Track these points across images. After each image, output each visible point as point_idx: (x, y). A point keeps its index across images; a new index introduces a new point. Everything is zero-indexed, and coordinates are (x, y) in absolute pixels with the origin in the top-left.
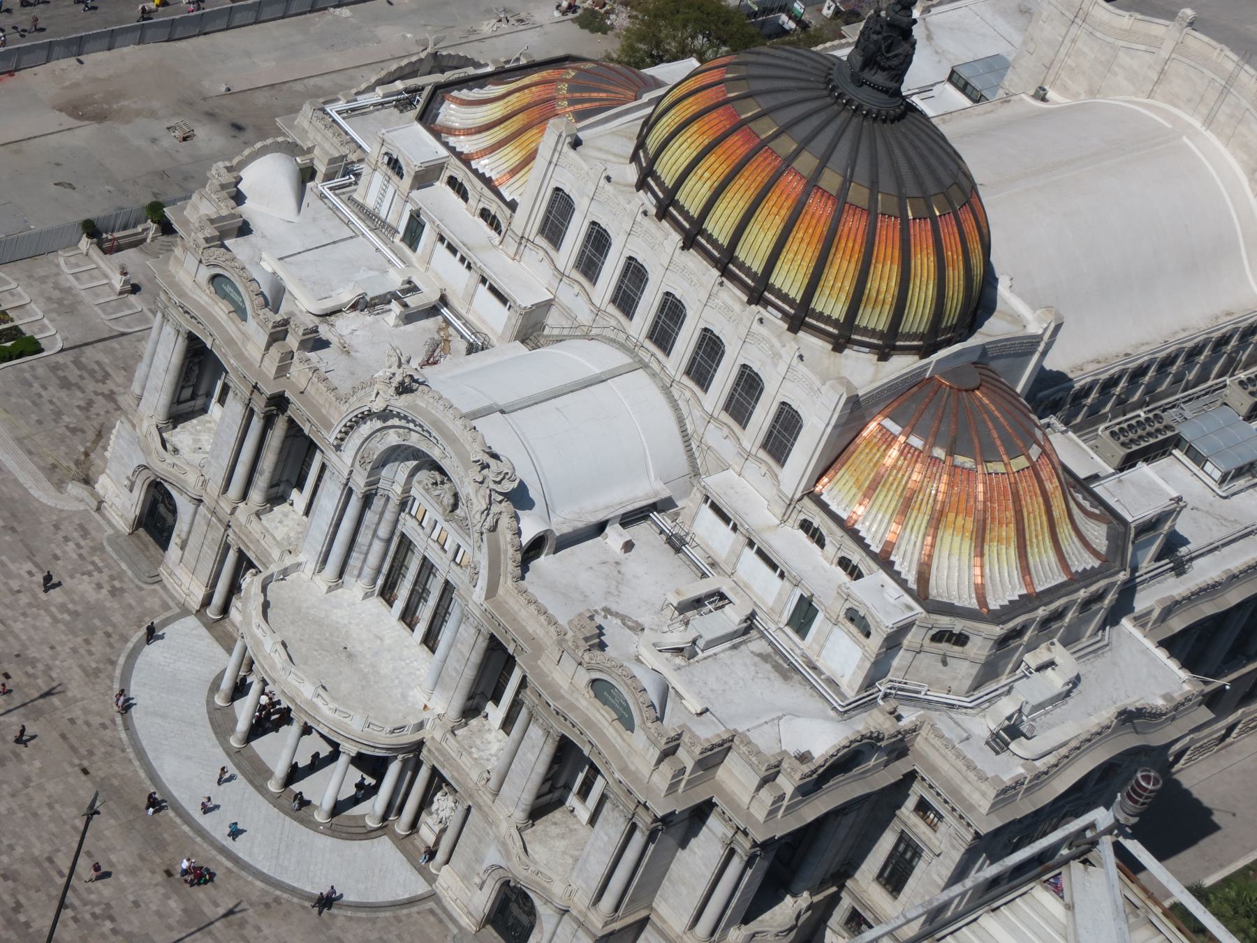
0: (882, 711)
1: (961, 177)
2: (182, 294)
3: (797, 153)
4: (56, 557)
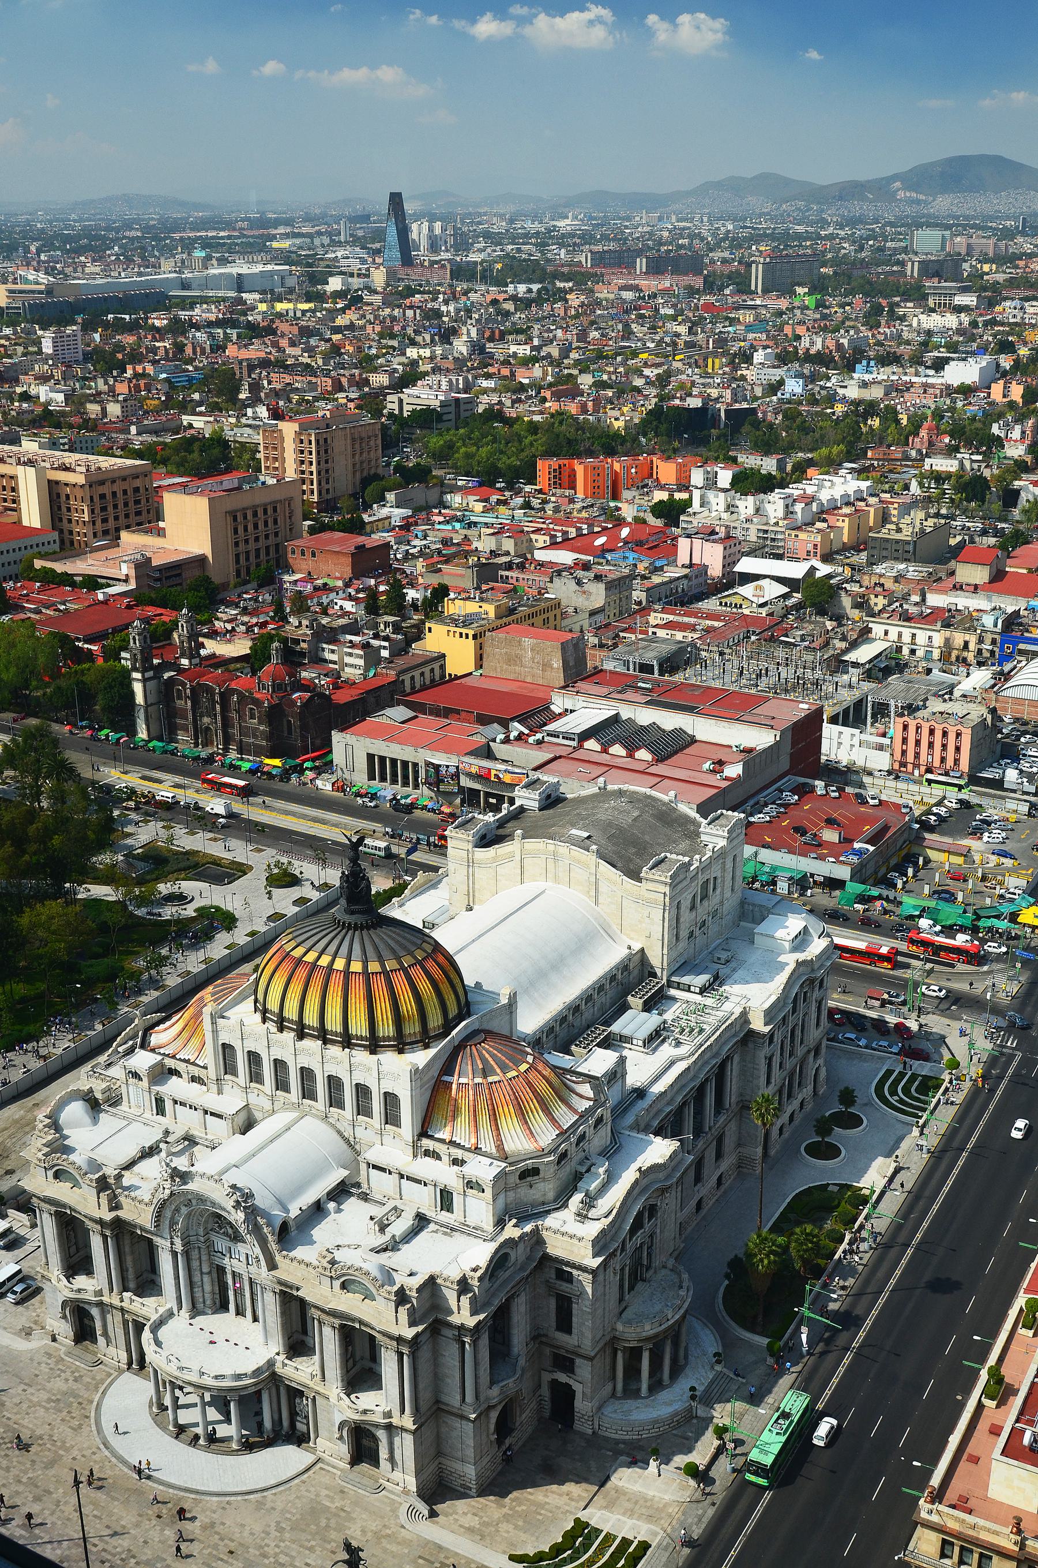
3: (333, 962)
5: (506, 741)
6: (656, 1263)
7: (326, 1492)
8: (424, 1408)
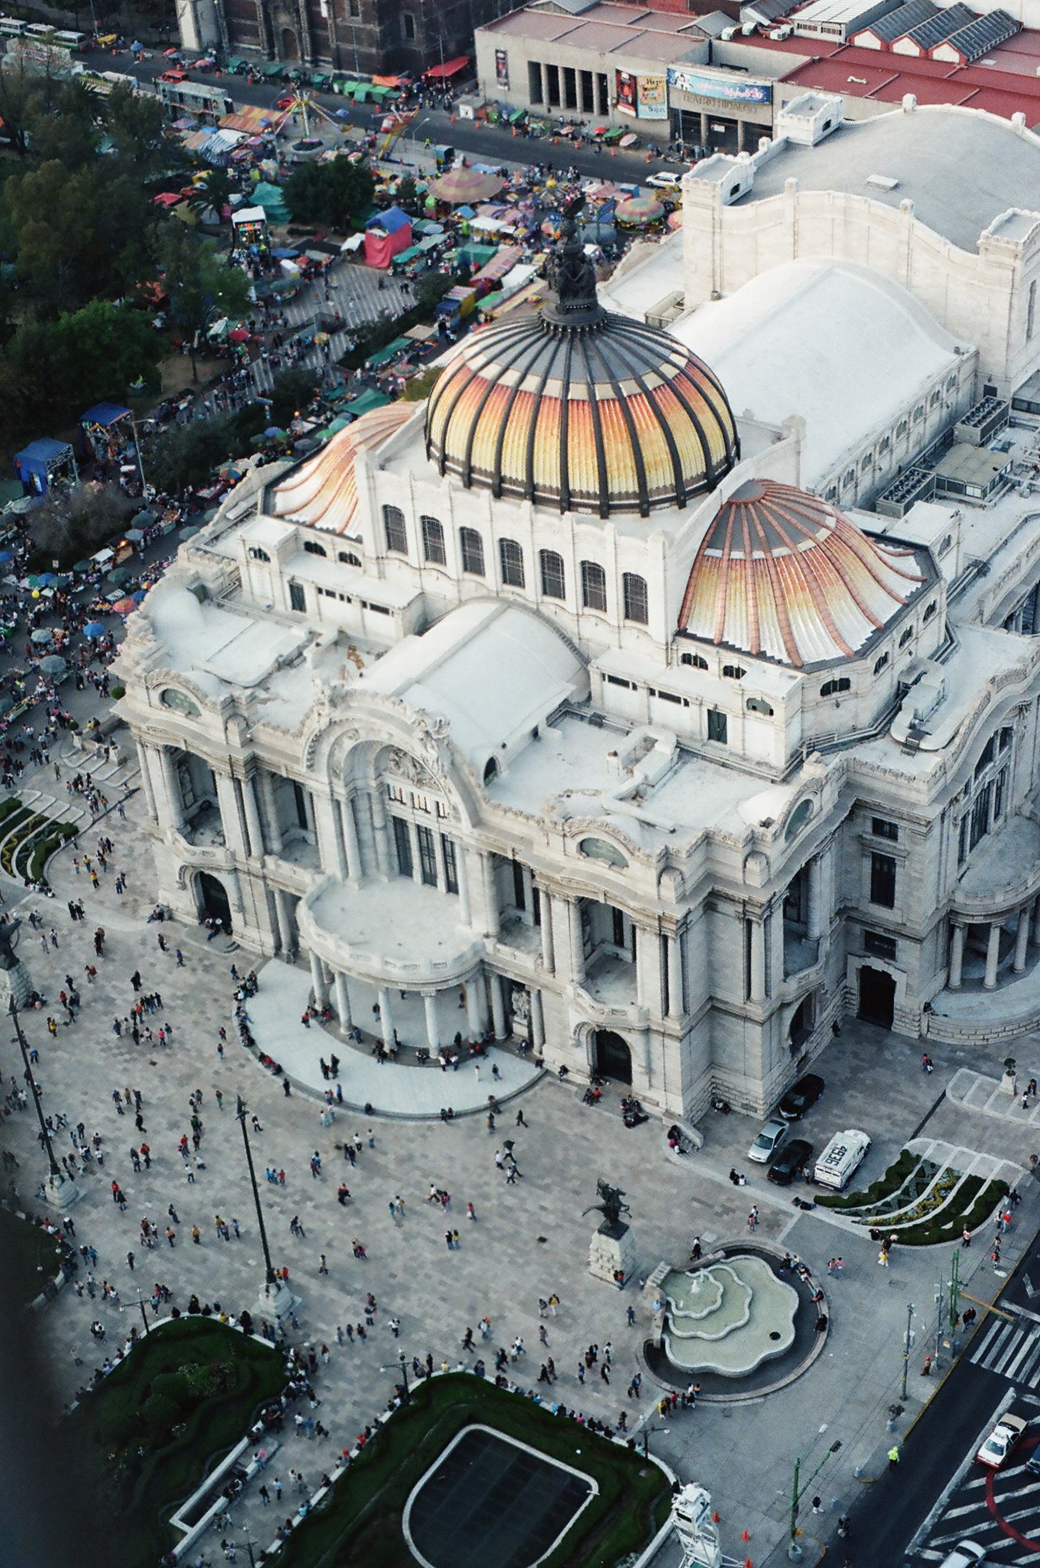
0: (810, 764)
1: (674, 345)
2: (146, 719)
4: (153, 965)
5: (738, 36)
6: (1008, 808)
7: (557, 1115)
8: (693, 1009)
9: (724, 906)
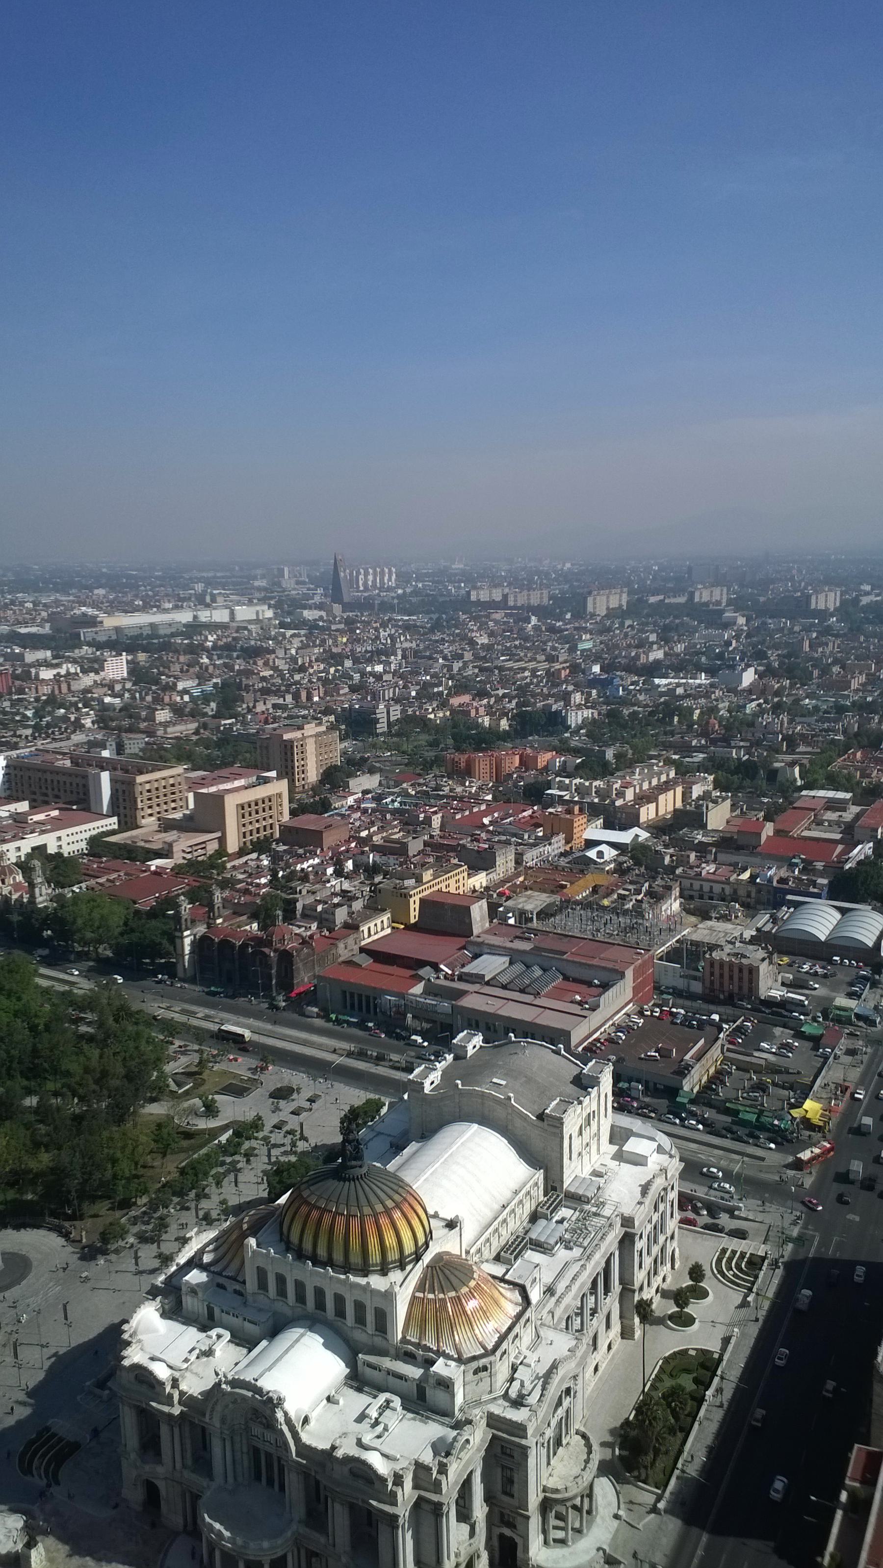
6: (573, 1432)
9: (426, 1506)
